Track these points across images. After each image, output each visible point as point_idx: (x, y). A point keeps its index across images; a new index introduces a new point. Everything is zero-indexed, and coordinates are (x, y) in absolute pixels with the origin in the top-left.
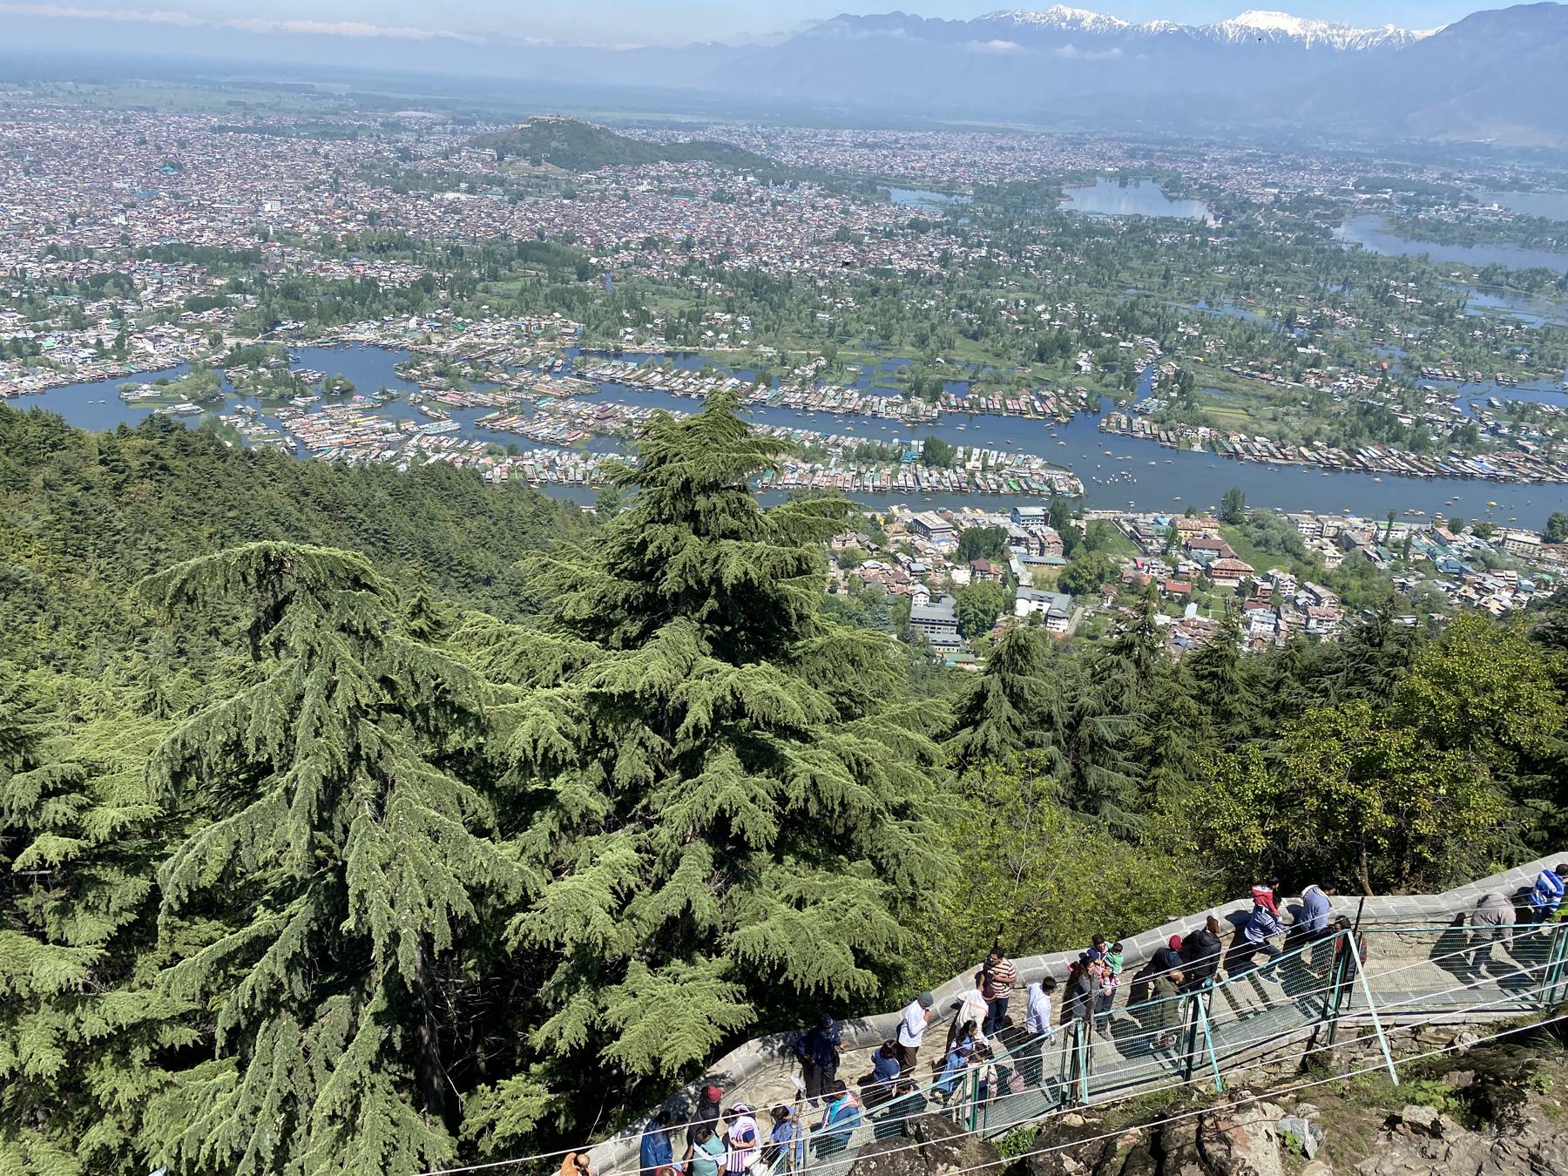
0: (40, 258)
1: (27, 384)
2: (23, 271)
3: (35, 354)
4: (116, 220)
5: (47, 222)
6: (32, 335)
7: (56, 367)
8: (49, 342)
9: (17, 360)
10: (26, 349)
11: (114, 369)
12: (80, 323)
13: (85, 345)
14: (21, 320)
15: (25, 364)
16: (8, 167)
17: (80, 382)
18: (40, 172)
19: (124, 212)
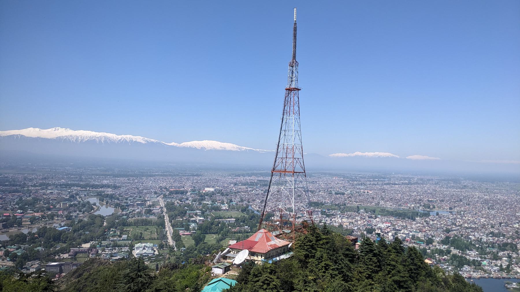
0: (487, 235)
1: (475, 275)
2: (481, 239)
3: (480, 266)
4: (515, 226)
5: (492, 225)
6: (479, 259)
7: (485, 271)
8: (485, 263)
9: (473, 267)
10: (477, 264)
11: (504, 275)
12: (496, 257)
13: (496, 265)
14: (477, 254)
15: (475, 268)
16: (483, 207)
17: (492, 278)
18: (493, 209)
19: (518, 223)
